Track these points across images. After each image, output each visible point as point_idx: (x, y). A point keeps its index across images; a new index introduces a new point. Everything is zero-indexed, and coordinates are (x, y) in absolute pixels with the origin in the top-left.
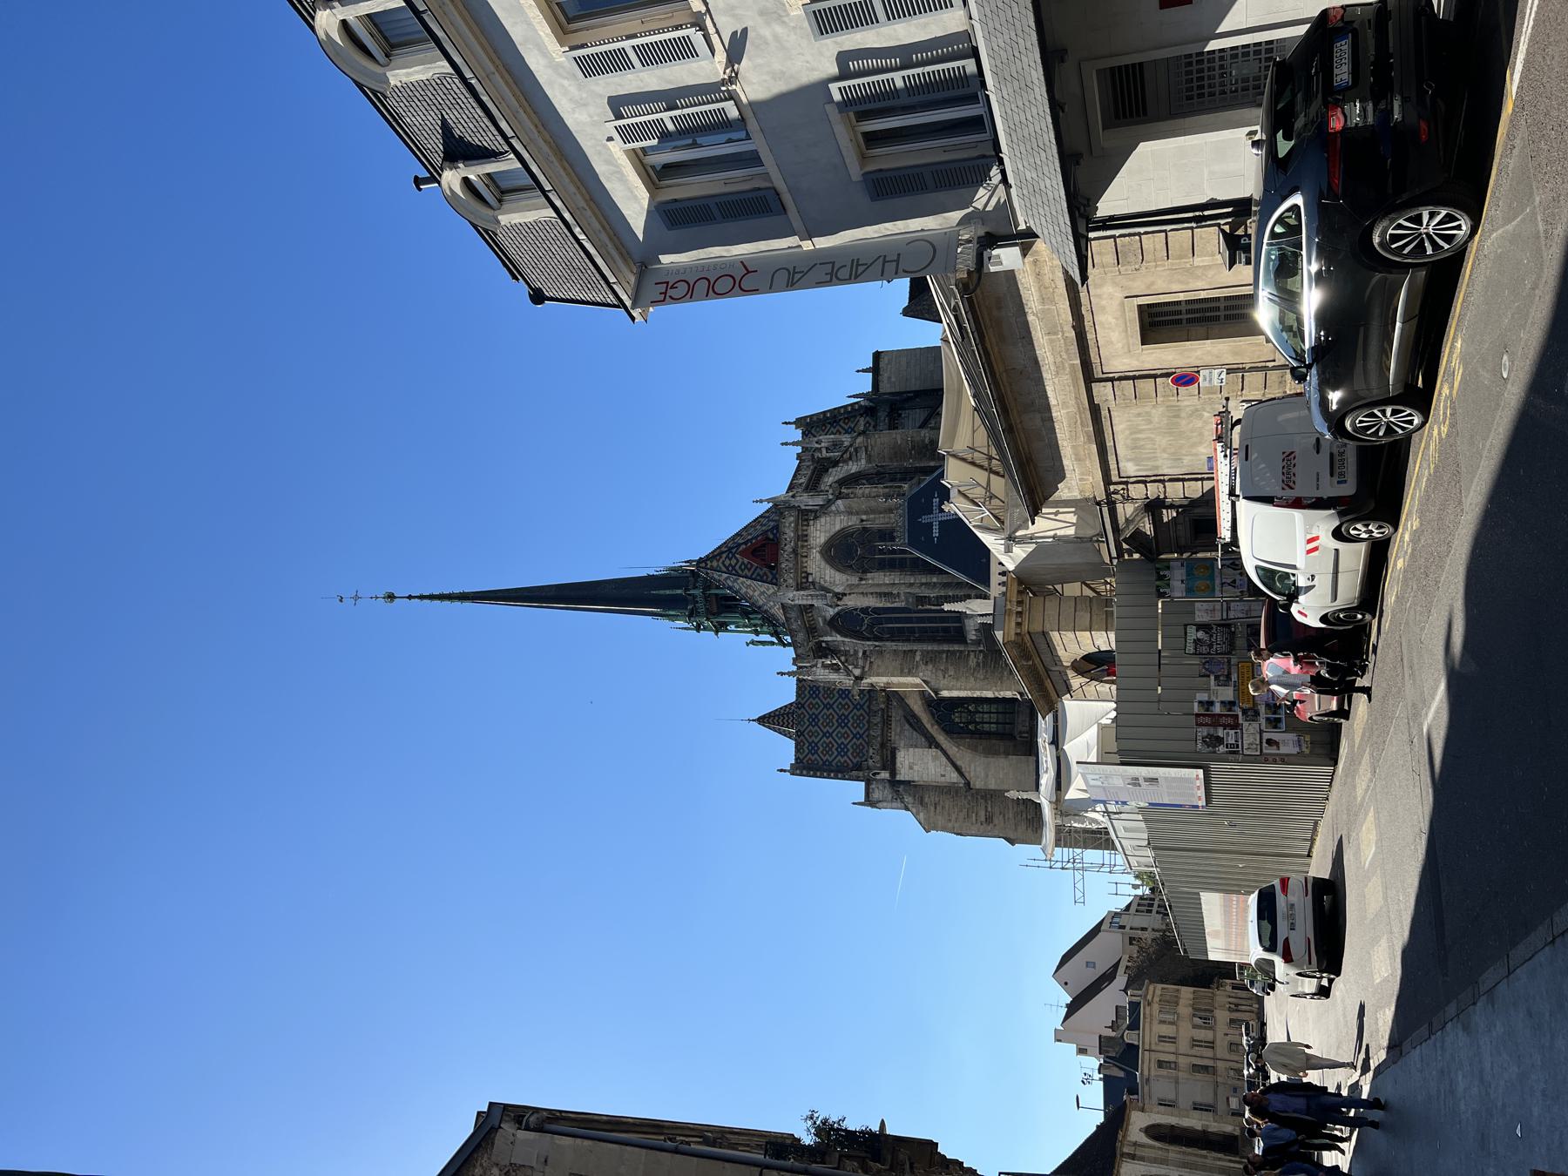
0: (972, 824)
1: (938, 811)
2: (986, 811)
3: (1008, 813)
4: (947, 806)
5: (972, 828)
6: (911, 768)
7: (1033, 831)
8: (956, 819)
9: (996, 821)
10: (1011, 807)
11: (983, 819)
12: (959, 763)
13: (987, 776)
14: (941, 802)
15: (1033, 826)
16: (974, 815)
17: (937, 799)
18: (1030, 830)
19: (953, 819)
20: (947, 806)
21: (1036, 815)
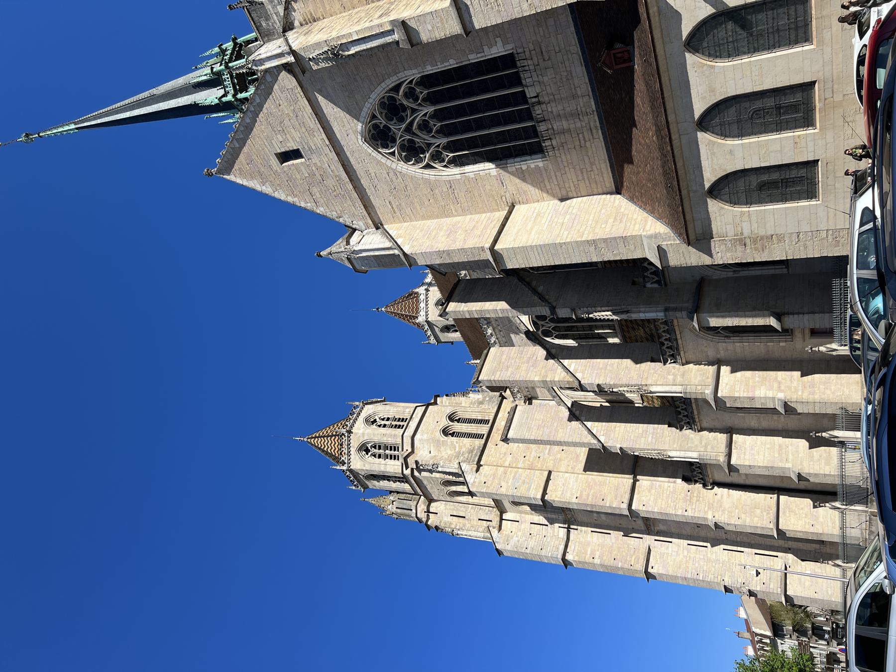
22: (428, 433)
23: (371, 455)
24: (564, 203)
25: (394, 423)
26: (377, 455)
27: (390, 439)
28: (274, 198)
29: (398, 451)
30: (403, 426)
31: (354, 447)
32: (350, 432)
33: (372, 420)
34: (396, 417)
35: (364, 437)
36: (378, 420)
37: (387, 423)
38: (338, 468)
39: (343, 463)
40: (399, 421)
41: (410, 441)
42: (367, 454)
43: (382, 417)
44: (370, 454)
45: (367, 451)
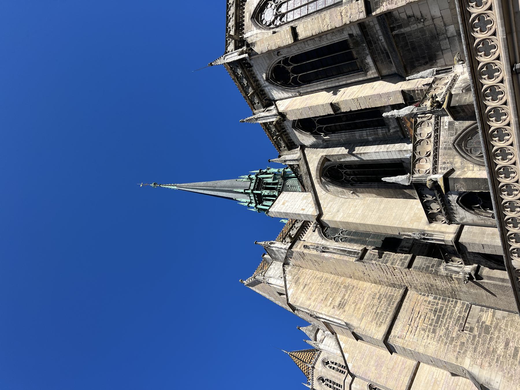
0: (326, 306)
1: (305, 290)
2: (342, 299)
3: (361, 303)
4: (313, 289)
5: (324, 309)
6: (283, 204)
7: (377, 324)
8: (315, 298)
9: (347, 308)
10: (365, 299)
11: (337, 304)
12: (321, 202)
13: (338, 211)
14: (311, 285)
15: (379, 319)
16: (331, 299)
17: (309, 281)
18: (374, 323)
19: (313, 298)
20: (313, 289)
21: (387, 310)
22: (359, 385)
23: (325, 384)
24: (453, 377)
25: (340, 368)
26: (329, 386)
27: (336, 380)
28: (275, 304)
29: (341, 388)
30: (345, 372)
31: (315, 377)
32: (313, 367)
33: (327, 361)
34: (341, 364)
35: (321, 373)
36: (330, 362)
37: (336, 367)
38: (306, 385)
39: (309, 383)
40: (342, 367)
41: (349, 386)
42: (323, 383)
43: (332, 361)
44: (325, 383)
45: (323, 381)
